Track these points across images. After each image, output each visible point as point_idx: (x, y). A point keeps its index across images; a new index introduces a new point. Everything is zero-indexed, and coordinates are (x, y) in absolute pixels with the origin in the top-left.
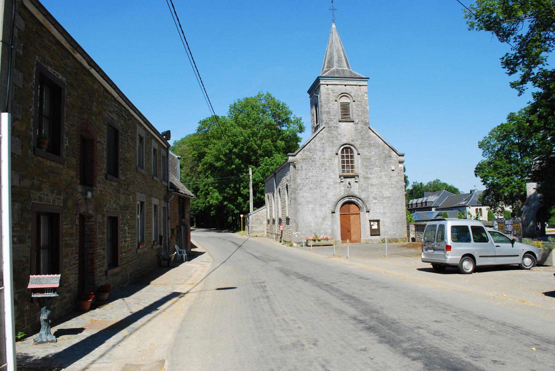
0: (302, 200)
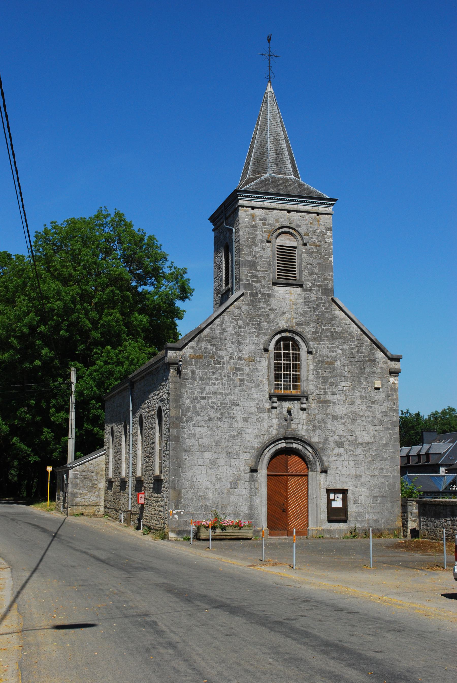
0: (192, 441)
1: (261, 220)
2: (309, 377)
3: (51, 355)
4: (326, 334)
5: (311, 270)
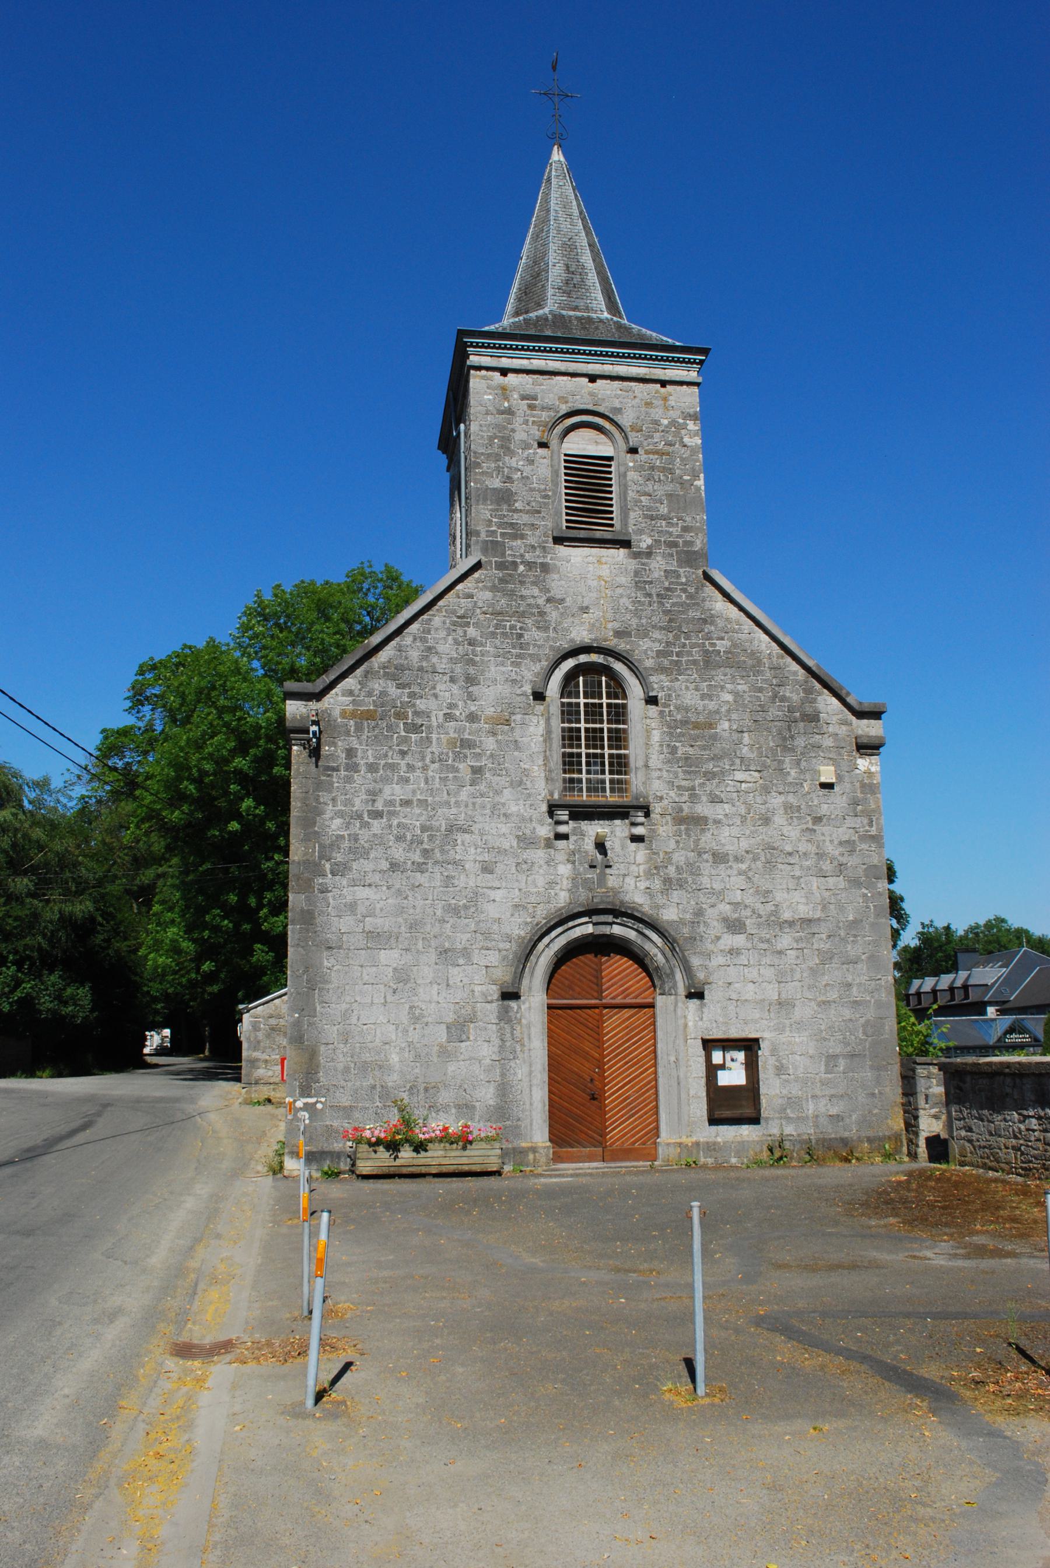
0: (346, 923)
1: (523, 398)
2: (651, 761)
3: (257, 811)
4: (692, 655)
5: (649, 509)
